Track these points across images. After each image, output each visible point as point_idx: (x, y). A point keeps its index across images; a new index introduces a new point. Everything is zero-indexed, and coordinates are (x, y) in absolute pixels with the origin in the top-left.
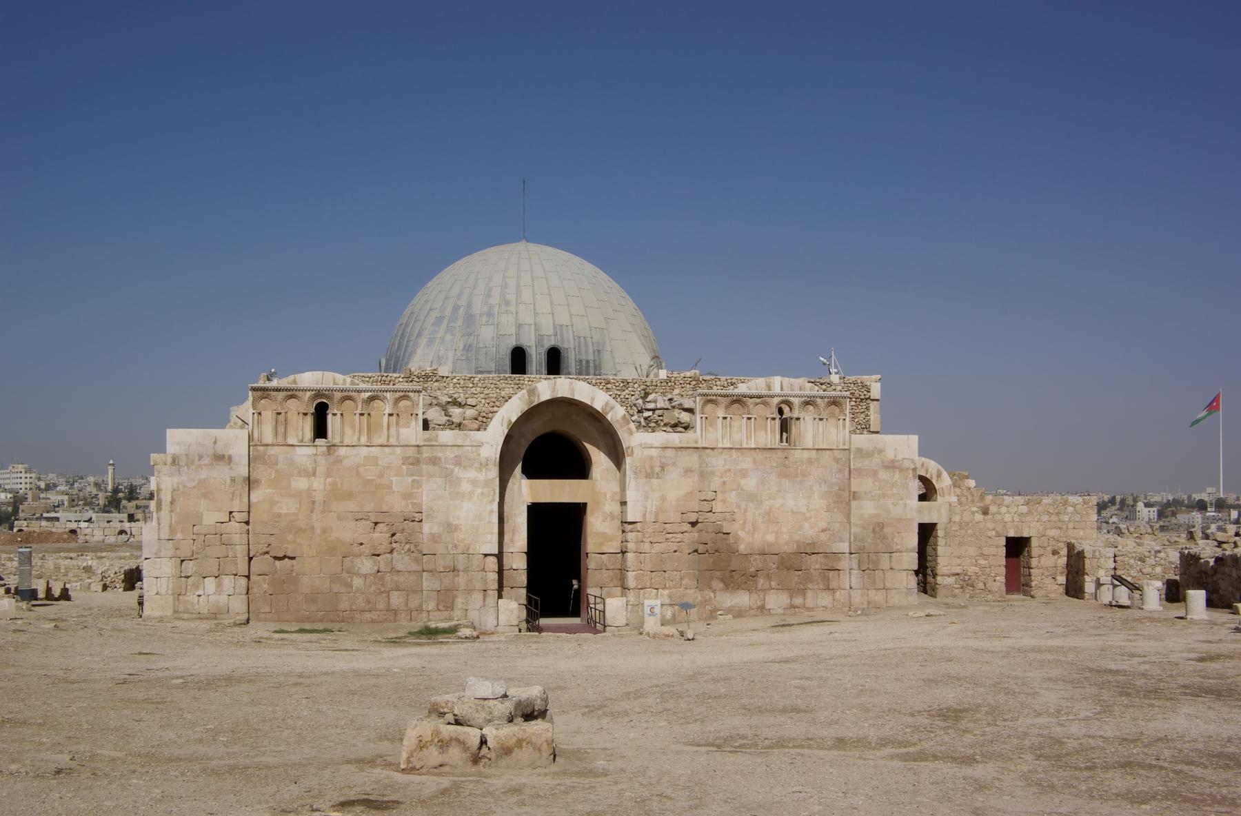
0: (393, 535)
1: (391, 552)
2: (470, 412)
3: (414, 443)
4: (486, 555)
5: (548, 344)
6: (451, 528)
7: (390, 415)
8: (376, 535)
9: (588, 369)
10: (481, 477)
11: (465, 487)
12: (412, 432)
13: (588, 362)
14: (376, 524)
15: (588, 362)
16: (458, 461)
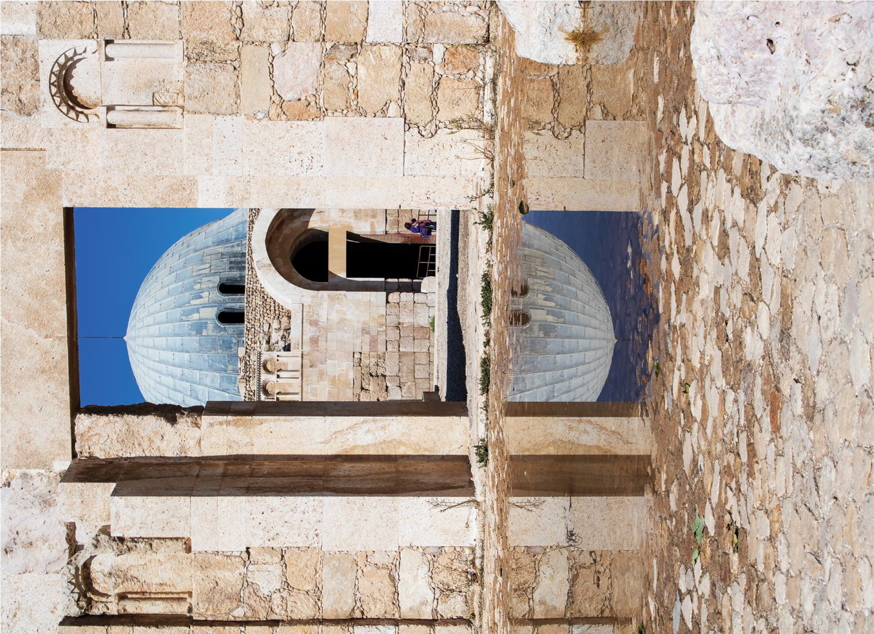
0: (371, 375)
1: (384, 376)
2: (275, 325)
3: (300, 359)
4: (387, 302)
5: (217, 295)
6: (365, 331)
7: (278, 377)
8: (371, 388)
9: (239, 261)
10: (325, 305)
11: (334, 317)
12: (291, 360)
13: (231, 263)
14: (362, 388)
15: (231, 263)
16: (314, 323)
